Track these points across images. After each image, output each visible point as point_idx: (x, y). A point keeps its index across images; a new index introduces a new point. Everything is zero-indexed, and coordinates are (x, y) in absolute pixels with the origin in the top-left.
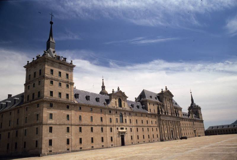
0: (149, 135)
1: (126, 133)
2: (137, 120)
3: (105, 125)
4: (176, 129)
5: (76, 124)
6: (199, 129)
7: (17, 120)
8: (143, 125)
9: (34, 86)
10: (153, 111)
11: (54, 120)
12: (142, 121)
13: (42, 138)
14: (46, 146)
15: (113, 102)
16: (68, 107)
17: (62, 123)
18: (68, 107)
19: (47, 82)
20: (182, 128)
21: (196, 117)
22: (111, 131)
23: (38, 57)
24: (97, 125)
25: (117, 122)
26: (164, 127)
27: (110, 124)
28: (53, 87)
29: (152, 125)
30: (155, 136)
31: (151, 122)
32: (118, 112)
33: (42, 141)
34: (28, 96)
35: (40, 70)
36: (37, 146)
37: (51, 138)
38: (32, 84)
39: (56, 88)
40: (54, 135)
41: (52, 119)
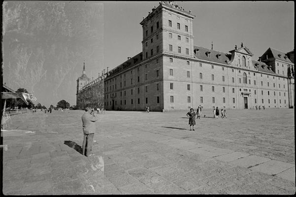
0: (275, 100)
8: (269, 88)
9: (152, 42)
10: (282, 73)
12: (268, 83)
15: (236, 60)
19: (165, 34)
22: (233, 92)
23: (153, 10)
27: (232, 84)
29: (280, 89)
30: (283, 102)
34: (147, 53)
35: (158, 23)
36: (158, 102)
38: (150, 40)
39: (176, 43)
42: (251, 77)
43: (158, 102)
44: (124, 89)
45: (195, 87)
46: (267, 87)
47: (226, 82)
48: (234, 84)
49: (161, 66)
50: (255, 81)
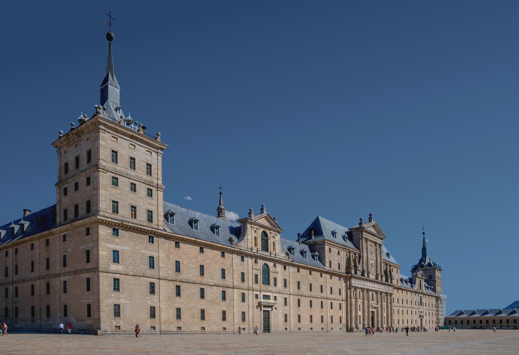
1: (274, 308)
2: (299, 282)
3: (232, 286)
5: (169, 278)
7: (45, 261)
8: (313, 294)
11: (122, 264)
12: (311, 284)
13: (99, 300)
14: (108, 317)
16: (151, 240)
17: (140, 272)
18: (151, 240)
24: (213, 284)
25: (257, 282)
29: (331, 296)
31: (329, 291)
32: (259, 260)
33: (99, 306)
36: (89, 315)
37: (117, 302)
40: (124, 296)
41: (119, 263)
42: (278, 272)
43: (89, 315)
44: (13, 283)
45: (165, 289)
46: (308, 293)
47: (228, 281)
48: (245, 285)
49: (96, 241)
50: (285, 280)
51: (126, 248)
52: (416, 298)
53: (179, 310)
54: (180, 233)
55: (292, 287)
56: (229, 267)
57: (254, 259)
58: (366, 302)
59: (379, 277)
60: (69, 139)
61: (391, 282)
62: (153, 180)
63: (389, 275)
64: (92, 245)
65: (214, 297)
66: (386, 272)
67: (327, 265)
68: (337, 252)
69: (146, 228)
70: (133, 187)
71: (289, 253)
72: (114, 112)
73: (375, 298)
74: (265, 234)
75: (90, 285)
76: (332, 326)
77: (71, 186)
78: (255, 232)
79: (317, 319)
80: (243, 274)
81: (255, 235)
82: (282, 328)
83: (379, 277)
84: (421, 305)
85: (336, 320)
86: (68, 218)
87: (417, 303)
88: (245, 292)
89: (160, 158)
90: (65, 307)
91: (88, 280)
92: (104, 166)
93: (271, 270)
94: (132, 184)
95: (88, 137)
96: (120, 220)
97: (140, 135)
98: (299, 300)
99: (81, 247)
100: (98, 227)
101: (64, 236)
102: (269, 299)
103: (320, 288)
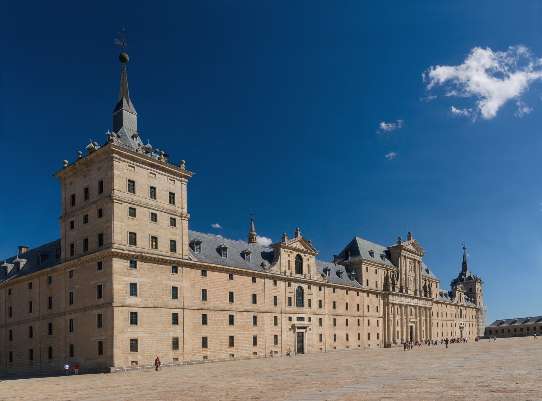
1: (308, 329)
2: (334, 302)
4: (420, 323)
6: (471, 325)
8: (349, 312)
12: (347, 304)
16: (175, 270)
17: (162, 304)
18: (175, 270)
20: (435, 323)
21: (468, 300)
25: (290, 304)
26: (394, 318)
28: (135, 222)
29: (368, 314)
32: (292, 283)
42: (312, 294)
46: (345, 312)
48: (278, 309)
50: (320, 301)
51: (146, 280)
52: (456, 310)
53: (205, 339)
54: (208, 261)
55: (328, 307)
56: (261, 292)
57: (287, 283)
58: (404, 317)
59: (418, 293)
60: (76, 169)
61: (430, 297)
62: (177, 209)
63: (428, 290)
64: (105, 279)
65: (244, 323)
66: (424, 287)
67: (364, 283)
68: (375, 271)
69: (169, 258)
70: (154, 217)
71: (325, 274)
72: (131, 139)
73: (413, 313)
74: (299, 258)
75: (104, 322)
76: (369, 343)
77: (78, 220)
78: (289, 255)
79: (353, 337)
80: (275, 298)
81: (288, 258)
82: (316, 349)
83: (418, 293)
84: (461, 317)
85: (373, 336)
86: (76, 253)
87: (457, 315)
88: (278, 315)
89: (185, 187)
90: (72, 347)
91: (100, 316)
92: (119, 197)
93: (305, 292)
94: (152, 214)
95: (99, 166)
96: (138, 252)
97: (161, 163)
98: (335, 319)
99: (91, 283)
100: (112, 260)
101: (71, 273)
102: (303, 320)
103: (357, 307)
